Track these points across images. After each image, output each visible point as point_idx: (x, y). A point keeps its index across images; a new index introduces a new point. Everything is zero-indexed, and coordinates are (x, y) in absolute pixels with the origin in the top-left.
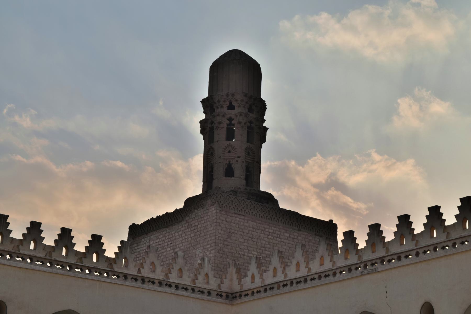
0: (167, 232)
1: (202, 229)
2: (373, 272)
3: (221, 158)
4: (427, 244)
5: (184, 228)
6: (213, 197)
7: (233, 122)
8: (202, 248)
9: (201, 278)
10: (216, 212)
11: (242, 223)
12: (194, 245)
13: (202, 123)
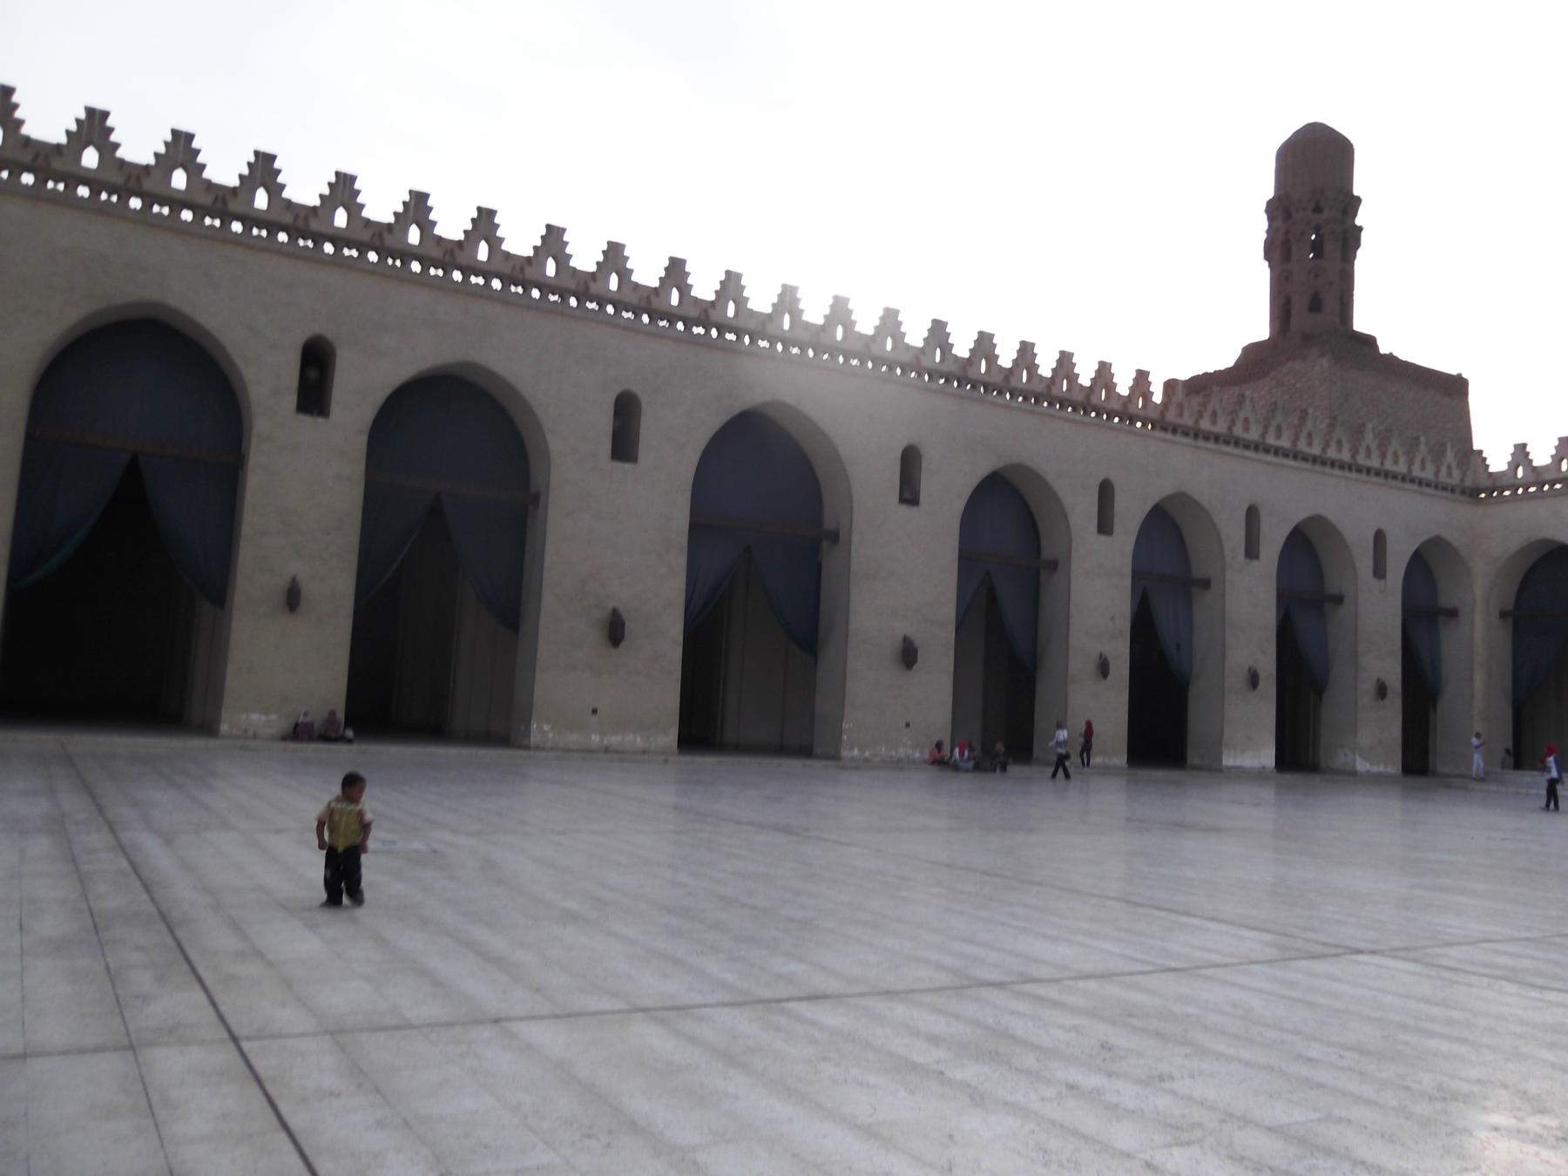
9: (1444, 470)
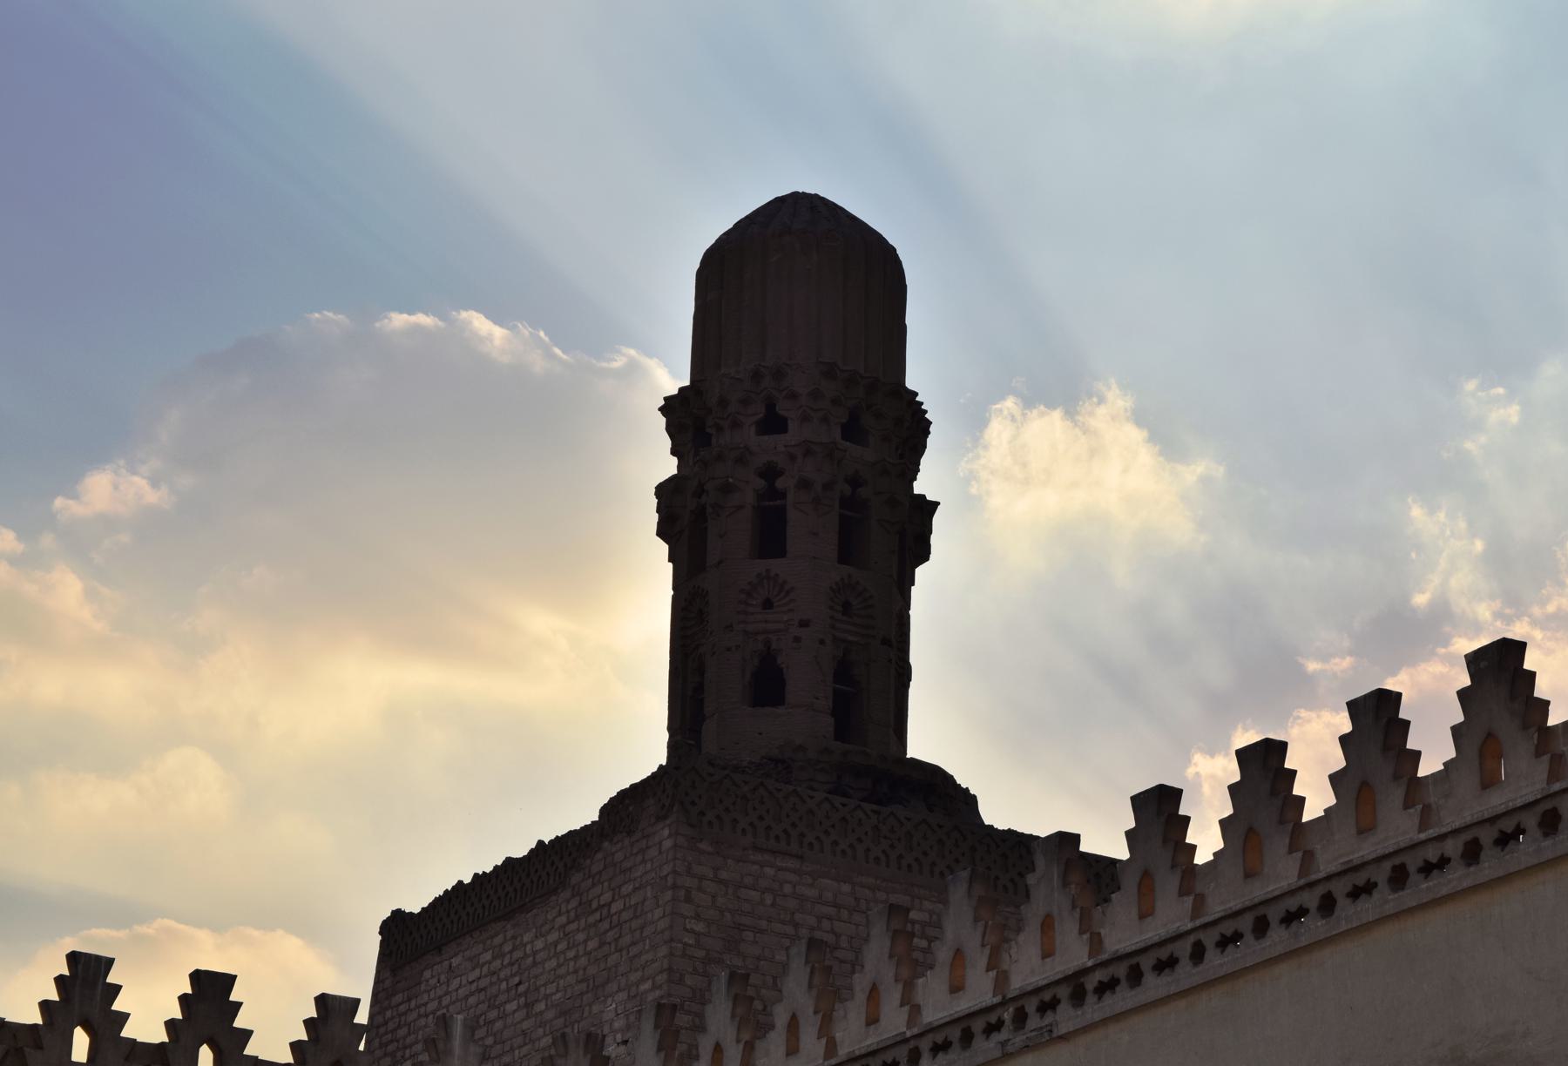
0: (508, 938)
1: (625, 916)
2: (1043, 1040)
3: (732, 631)
4: (1231, 908)
5: (563, 919)
6: (664, 784)
7: (780, 483)
8: (622, 996)
10: (675, 845)
11: (787, 889)
12: (596, 984)
13: (663, 491)
